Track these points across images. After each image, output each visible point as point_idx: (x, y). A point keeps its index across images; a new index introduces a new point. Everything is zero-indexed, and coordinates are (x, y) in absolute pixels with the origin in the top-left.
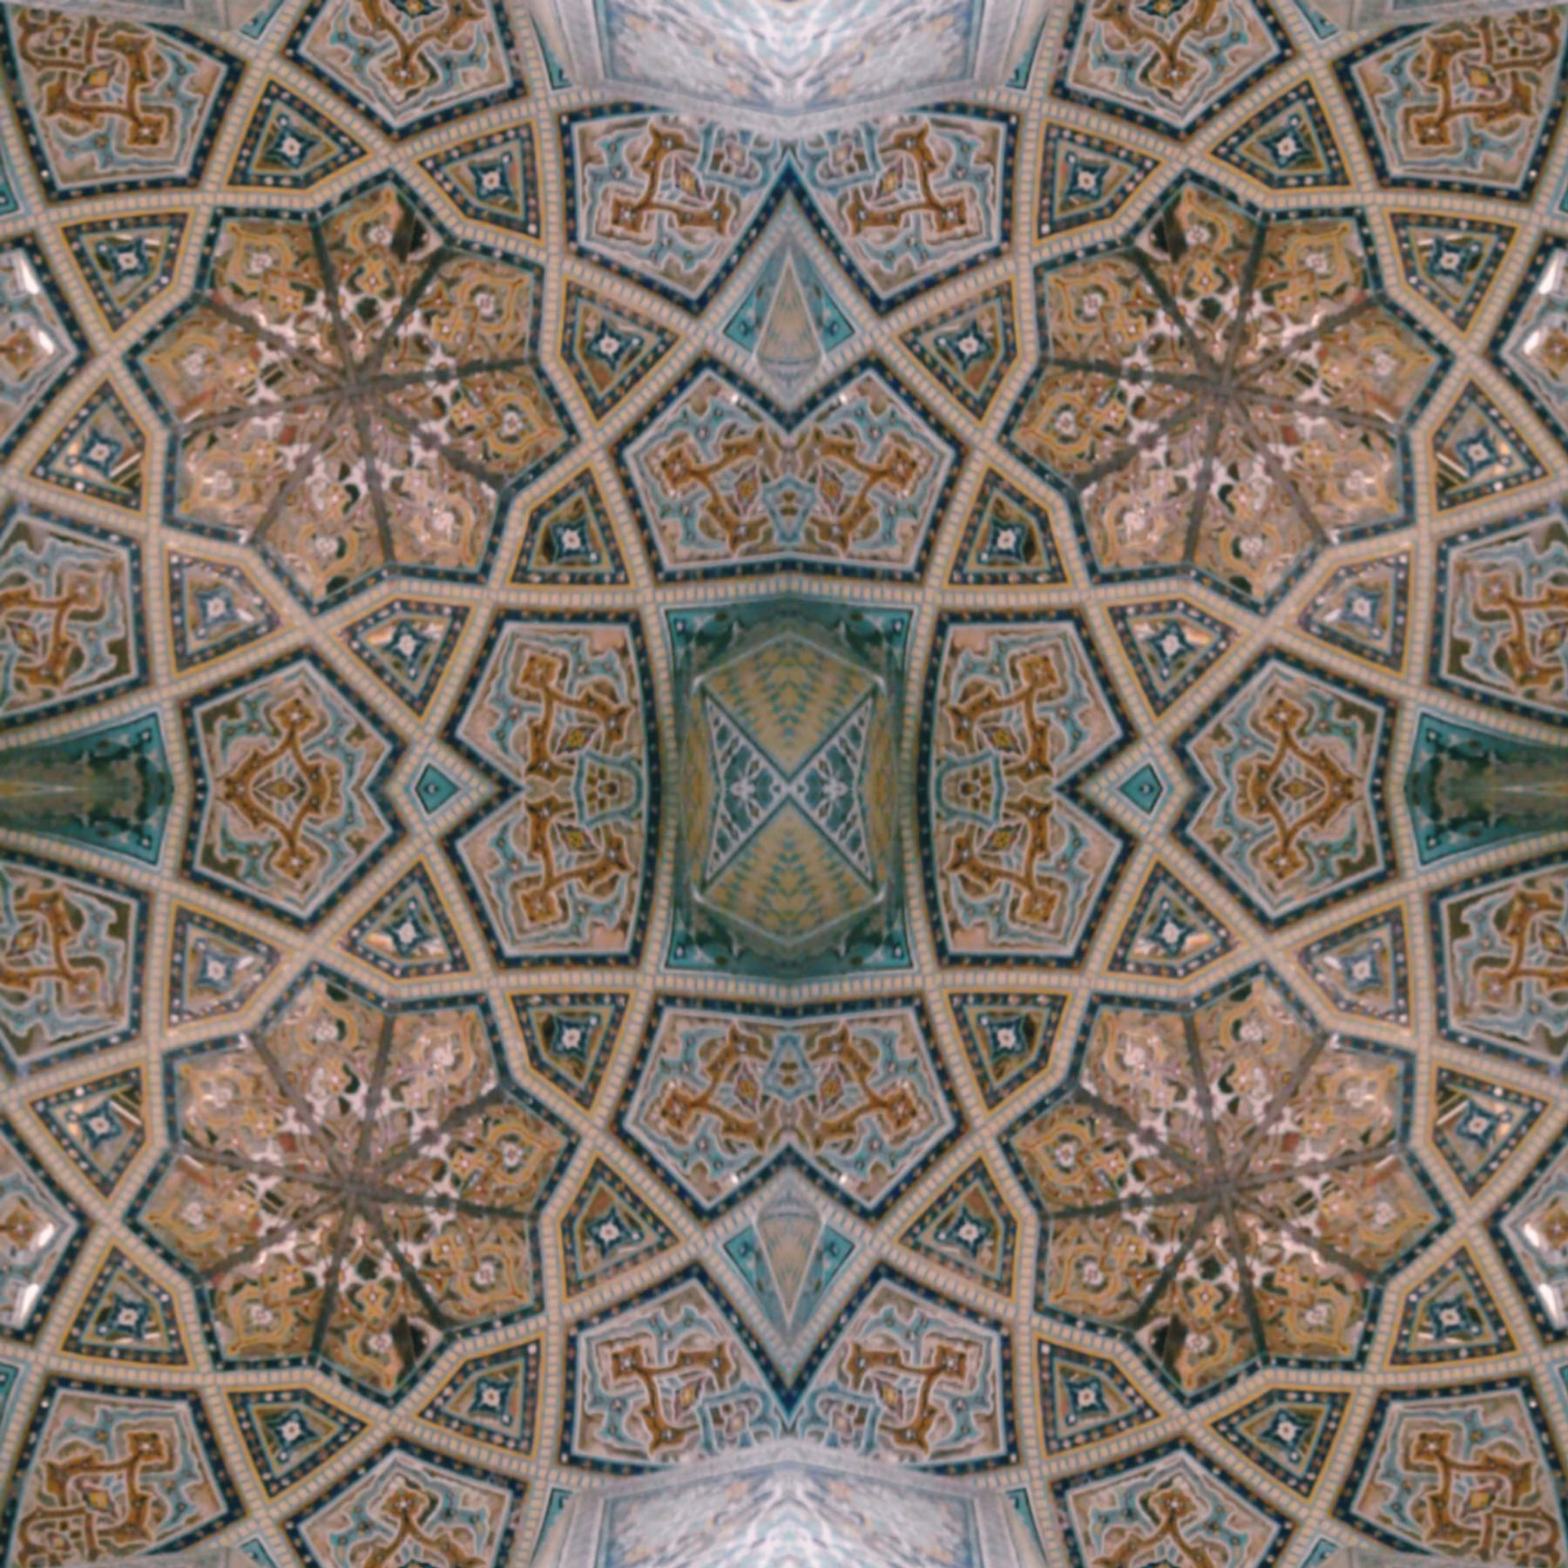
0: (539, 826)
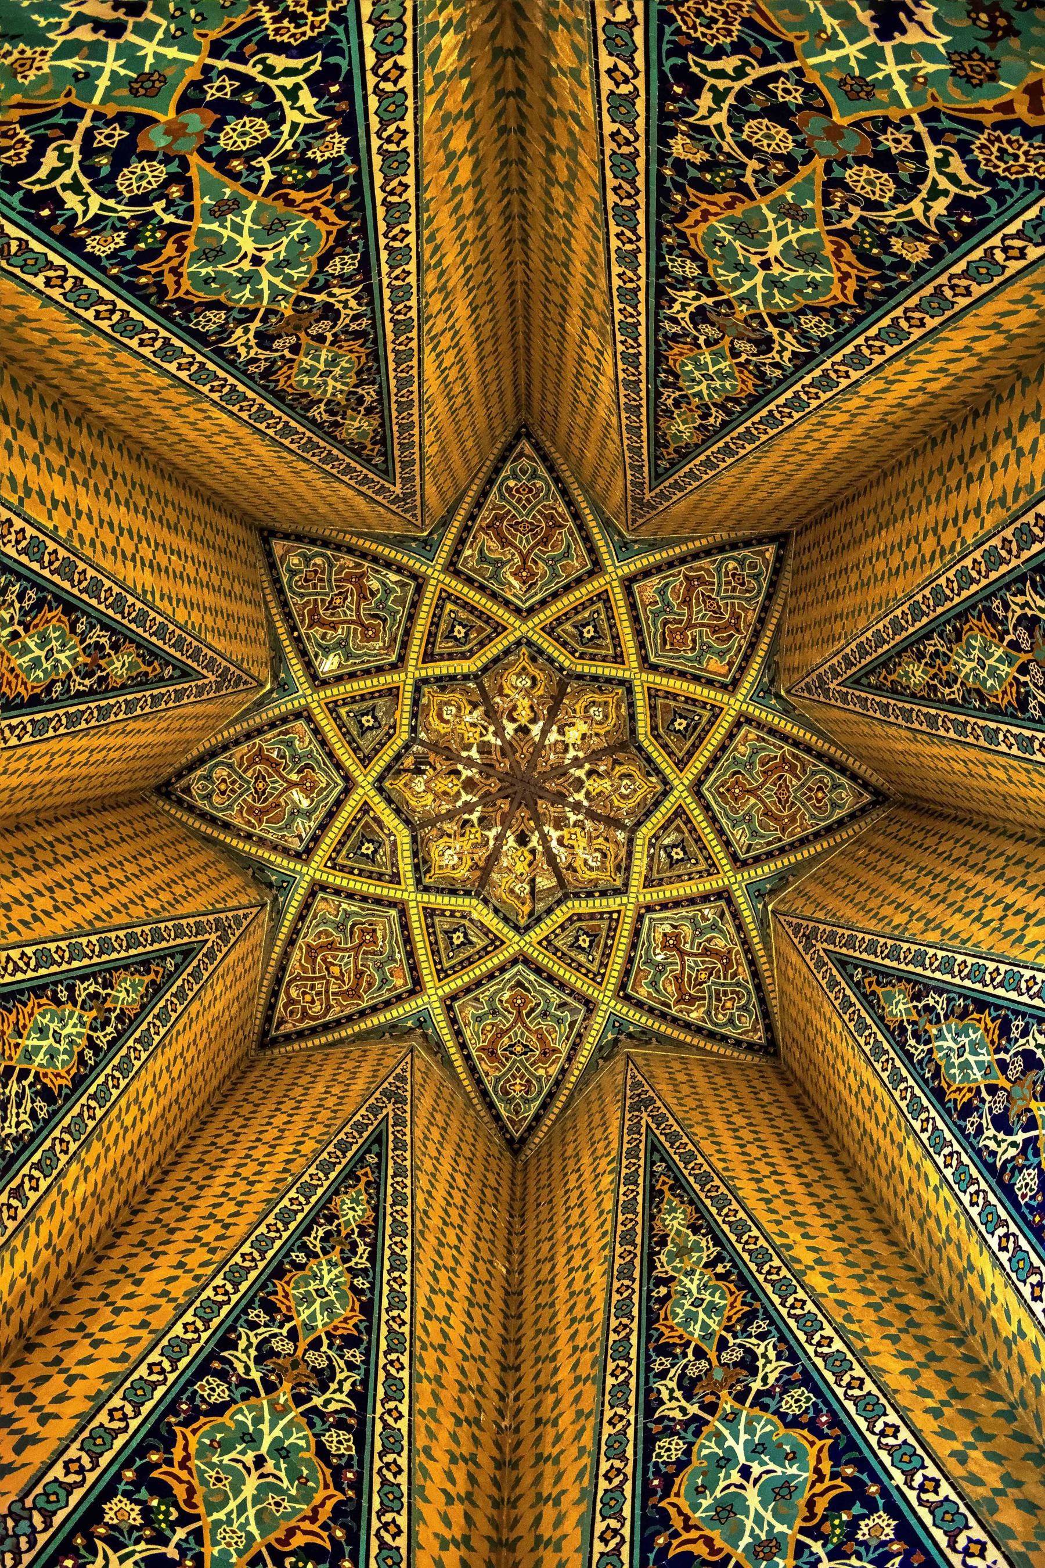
0: (689, 590)
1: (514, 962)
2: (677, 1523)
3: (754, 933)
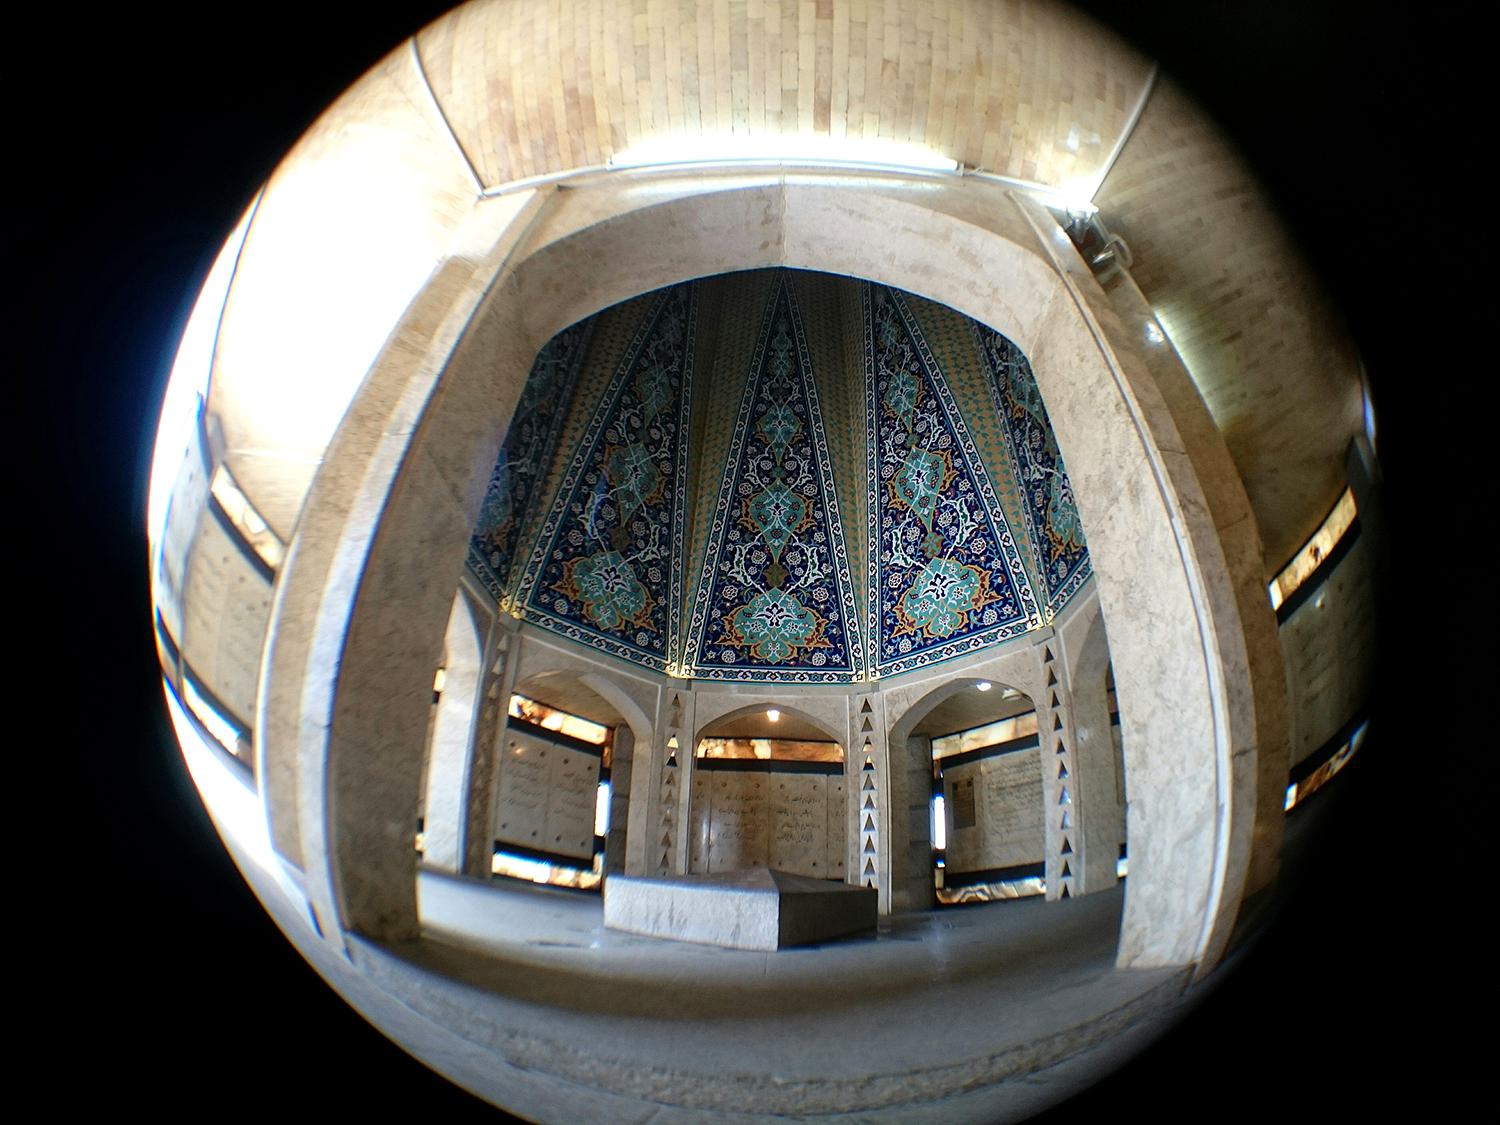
2: (759, 429)
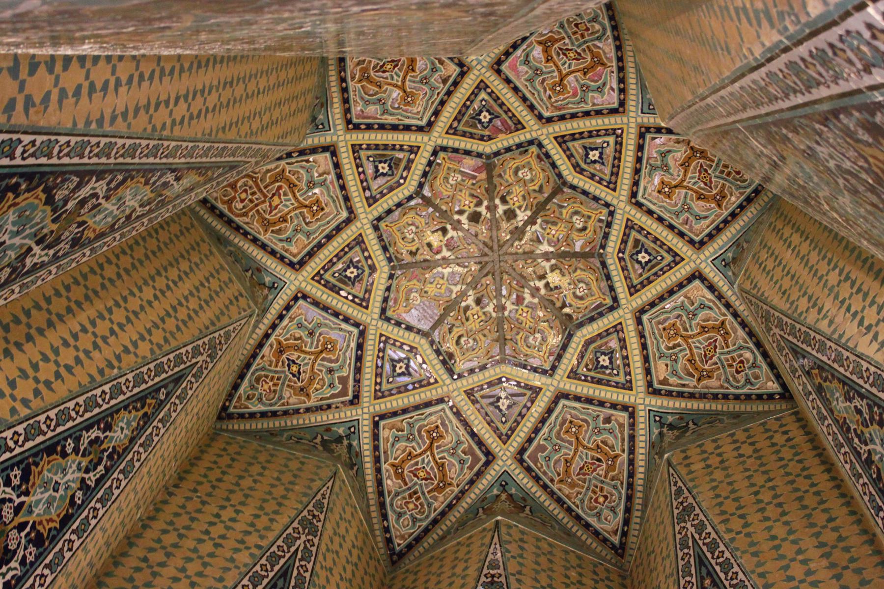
1: (357, 325)
3: (473, 496)
